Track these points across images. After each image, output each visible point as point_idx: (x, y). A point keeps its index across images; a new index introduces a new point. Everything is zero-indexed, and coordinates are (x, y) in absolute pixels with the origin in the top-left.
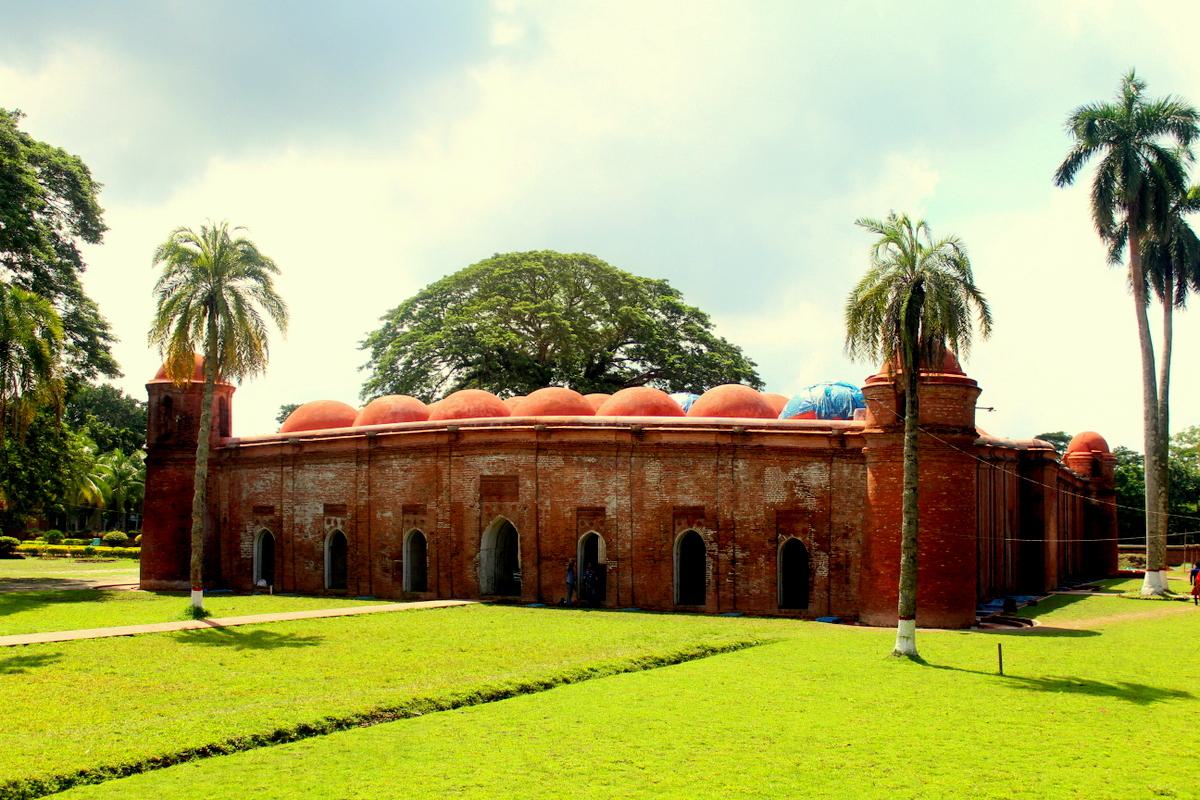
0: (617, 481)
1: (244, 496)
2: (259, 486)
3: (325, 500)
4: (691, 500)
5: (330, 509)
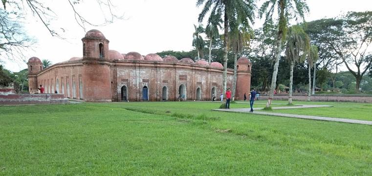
0: (204, 77)
1: (118, 76)
2: (123, 73)
3: (143, 78)
4: (214, 82)
5: (144, 81)
